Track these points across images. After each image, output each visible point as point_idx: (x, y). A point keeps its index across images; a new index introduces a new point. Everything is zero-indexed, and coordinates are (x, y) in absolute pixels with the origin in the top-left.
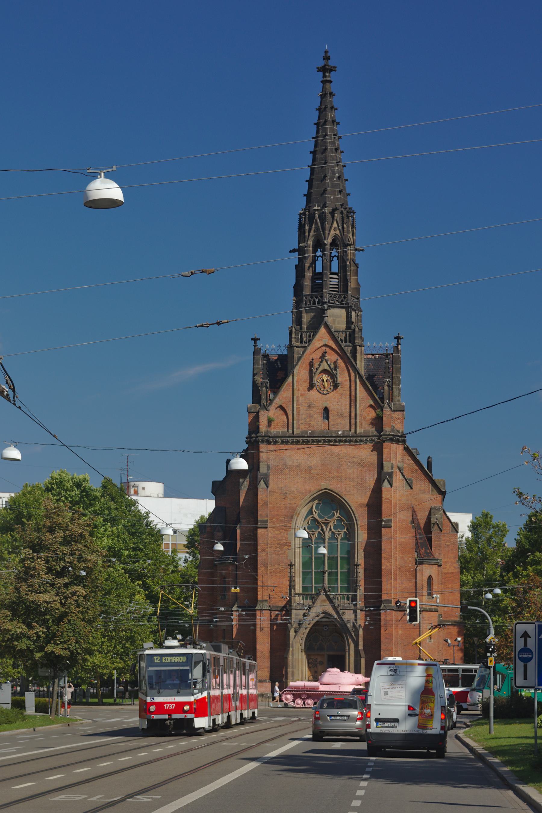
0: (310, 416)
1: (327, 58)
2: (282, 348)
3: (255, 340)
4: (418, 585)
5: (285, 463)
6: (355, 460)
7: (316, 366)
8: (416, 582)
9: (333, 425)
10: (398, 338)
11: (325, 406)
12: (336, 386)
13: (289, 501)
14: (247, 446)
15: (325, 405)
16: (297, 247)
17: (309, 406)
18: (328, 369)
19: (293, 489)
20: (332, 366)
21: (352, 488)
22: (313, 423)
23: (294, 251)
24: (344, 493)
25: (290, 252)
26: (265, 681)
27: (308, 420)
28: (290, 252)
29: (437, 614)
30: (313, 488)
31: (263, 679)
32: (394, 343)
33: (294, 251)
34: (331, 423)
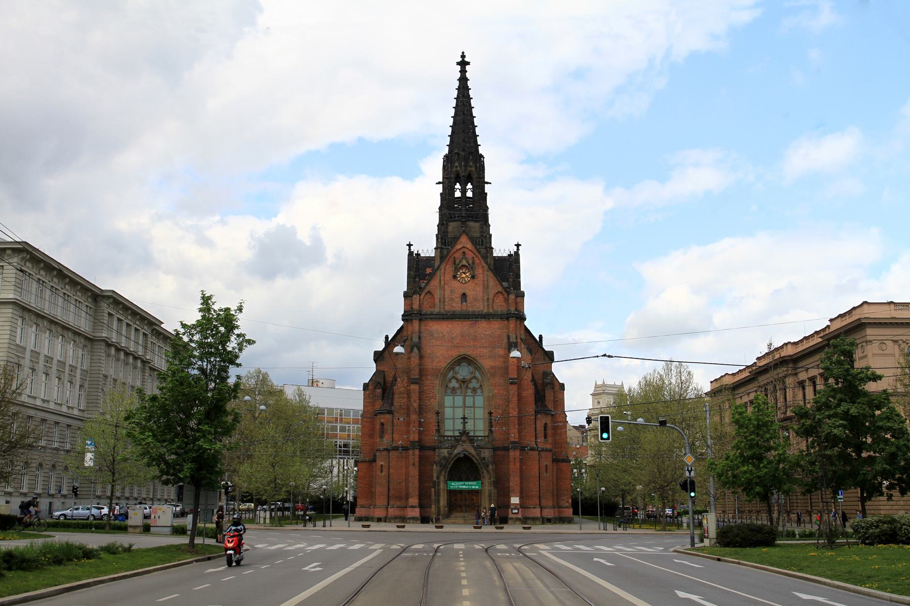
0: (452, 300)
1: (463, 56)
2: (430, 252)
3: (410, 245)
4: (537, 430)
5: (432, 335)
6: (487, 333)
7: (457, 262)
8: (536, 428)
9: (470, 306)
10: (518, 245)
11: (462, 293)
12: (473, 277)
13: (435, 364)
14: (402, 323)
15: (463, 291)
16: (441, 181)
17: (451, 292)
18: (467, 264)
19: (438, 355)
20: (470, 262)
21: (485, 354)
22: (455, 305)
23: (439, 183)
24: (479, 358)
25: (437, 183)
26: (415, 507)
27: (450, 302)
28: (437, 183)
29: (551, 453)
30: (454, 355)
31: (414, 505)
32: (515, 248)
33: (439, 183)
34: (469, 305)
